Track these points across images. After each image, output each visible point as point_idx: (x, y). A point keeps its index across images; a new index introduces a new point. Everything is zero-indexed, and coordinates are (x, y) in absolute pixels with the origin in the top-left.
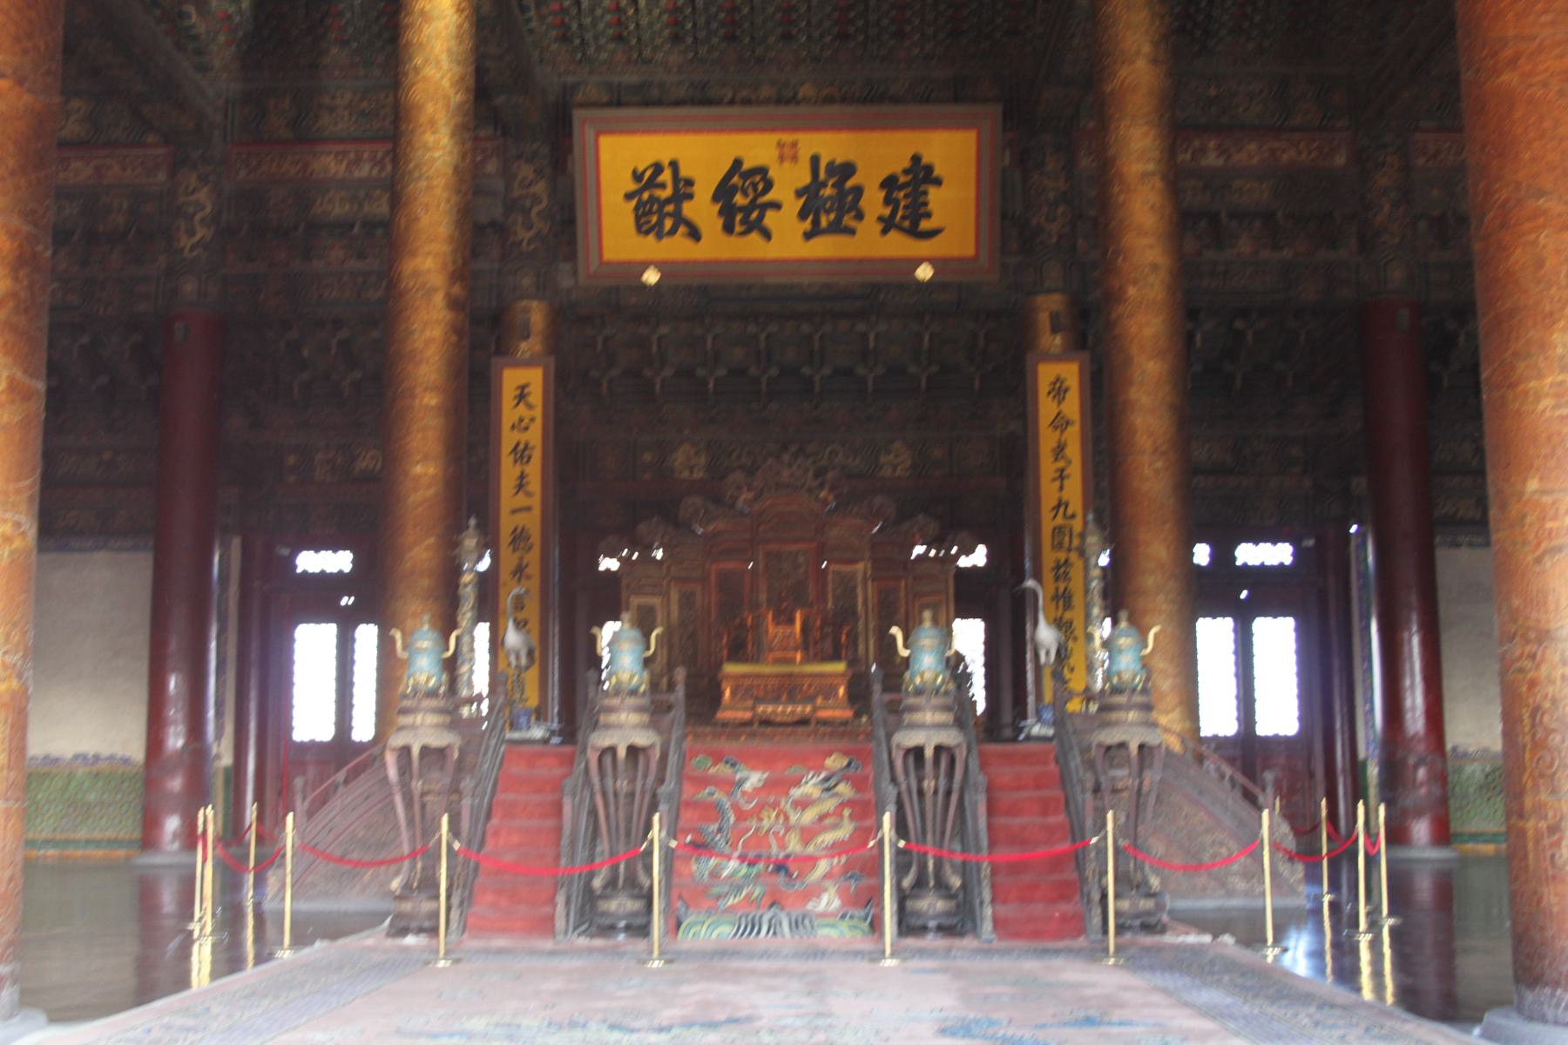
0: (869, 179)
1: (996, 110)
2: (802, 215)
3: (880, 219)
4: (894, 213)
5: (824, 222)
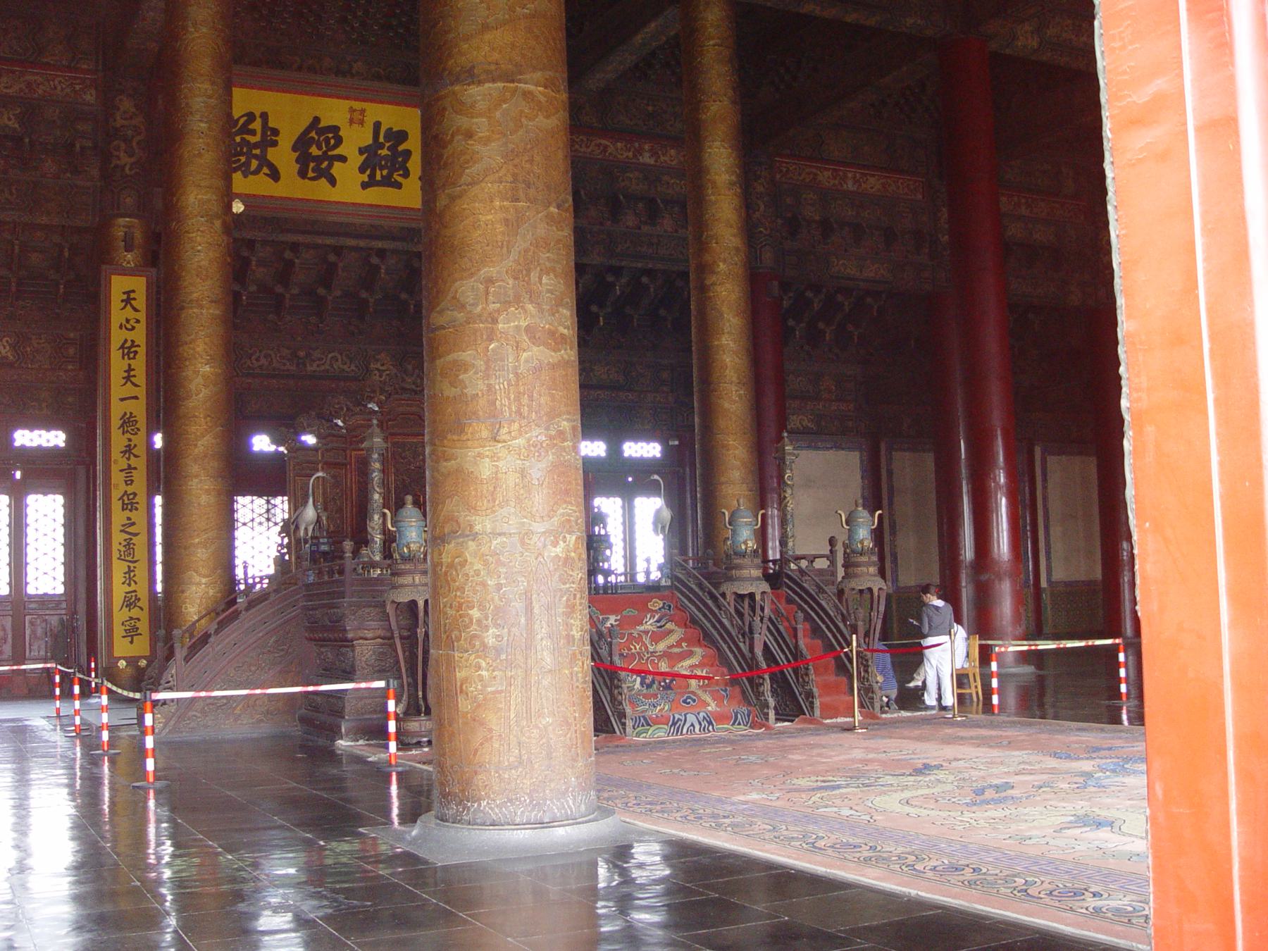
2: (362, 170)
5: (378, 177)
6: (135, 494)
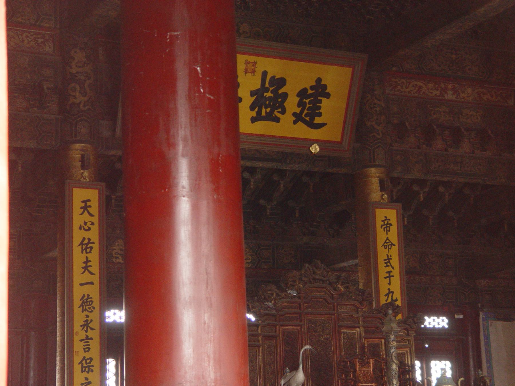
0: (292, 89)
2: (252, 108)
3: (294, 114)
4: (302, 112)
5: (263, 114)
6: (91, 359)
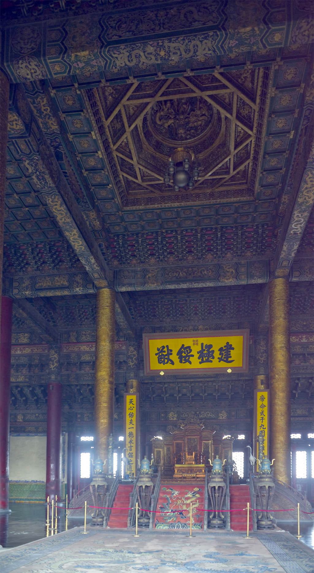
0: (216, 349)
1: (248, 330)
2: (199, 358)
3: (219, 358)
4: (222, 357)
